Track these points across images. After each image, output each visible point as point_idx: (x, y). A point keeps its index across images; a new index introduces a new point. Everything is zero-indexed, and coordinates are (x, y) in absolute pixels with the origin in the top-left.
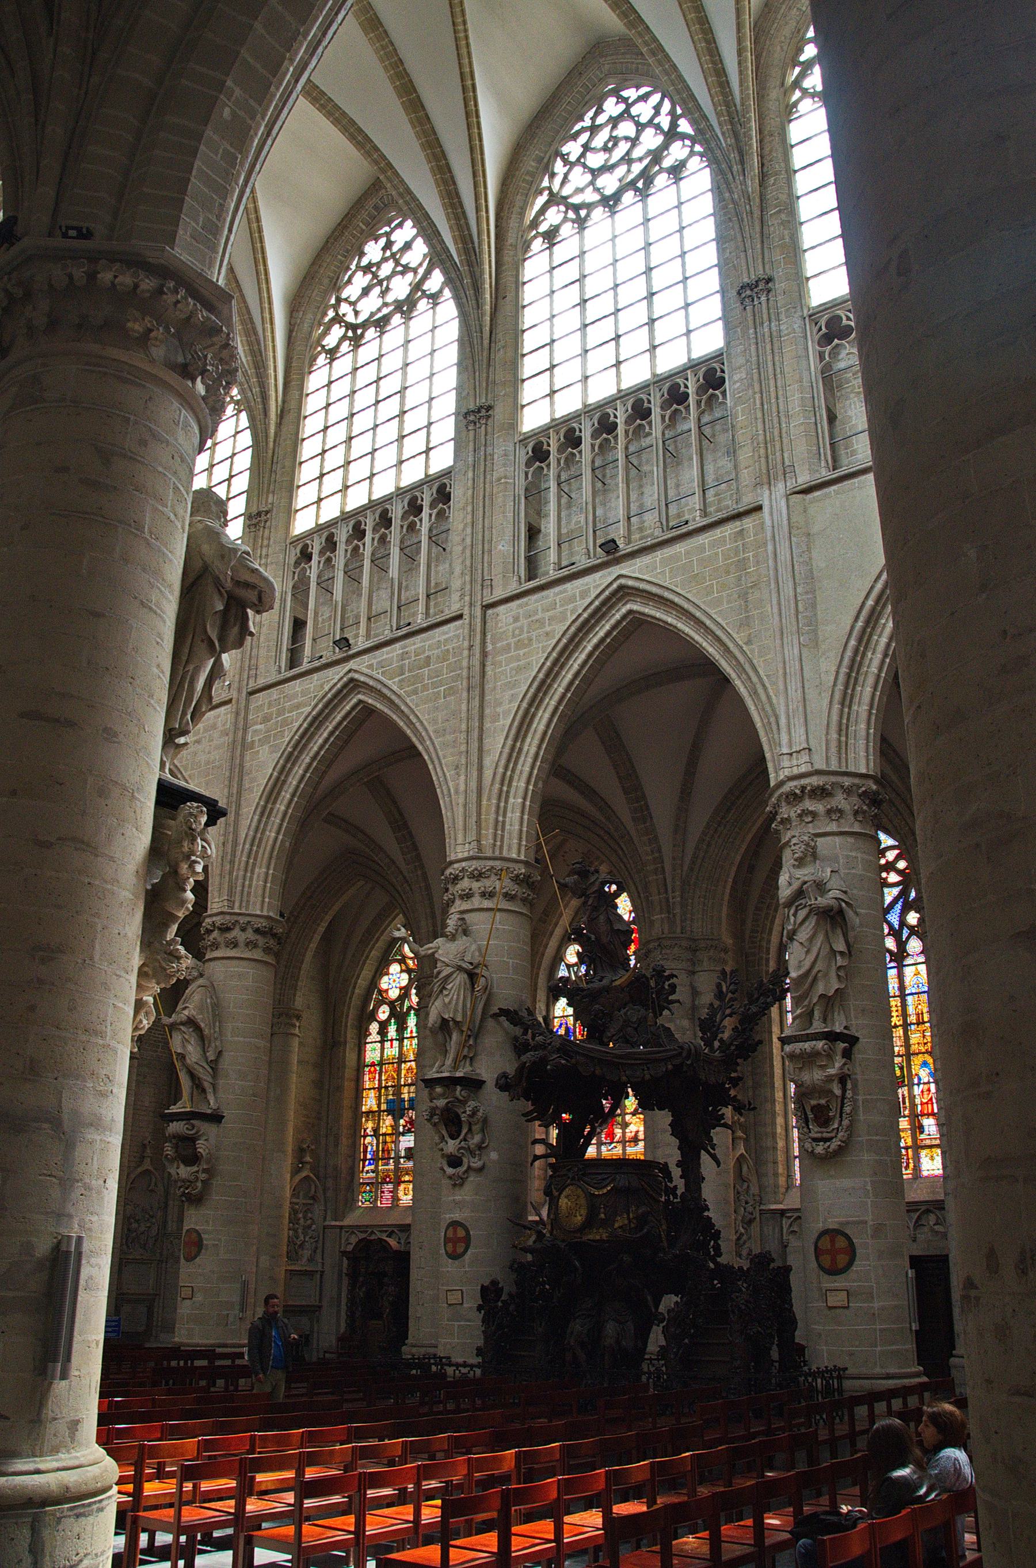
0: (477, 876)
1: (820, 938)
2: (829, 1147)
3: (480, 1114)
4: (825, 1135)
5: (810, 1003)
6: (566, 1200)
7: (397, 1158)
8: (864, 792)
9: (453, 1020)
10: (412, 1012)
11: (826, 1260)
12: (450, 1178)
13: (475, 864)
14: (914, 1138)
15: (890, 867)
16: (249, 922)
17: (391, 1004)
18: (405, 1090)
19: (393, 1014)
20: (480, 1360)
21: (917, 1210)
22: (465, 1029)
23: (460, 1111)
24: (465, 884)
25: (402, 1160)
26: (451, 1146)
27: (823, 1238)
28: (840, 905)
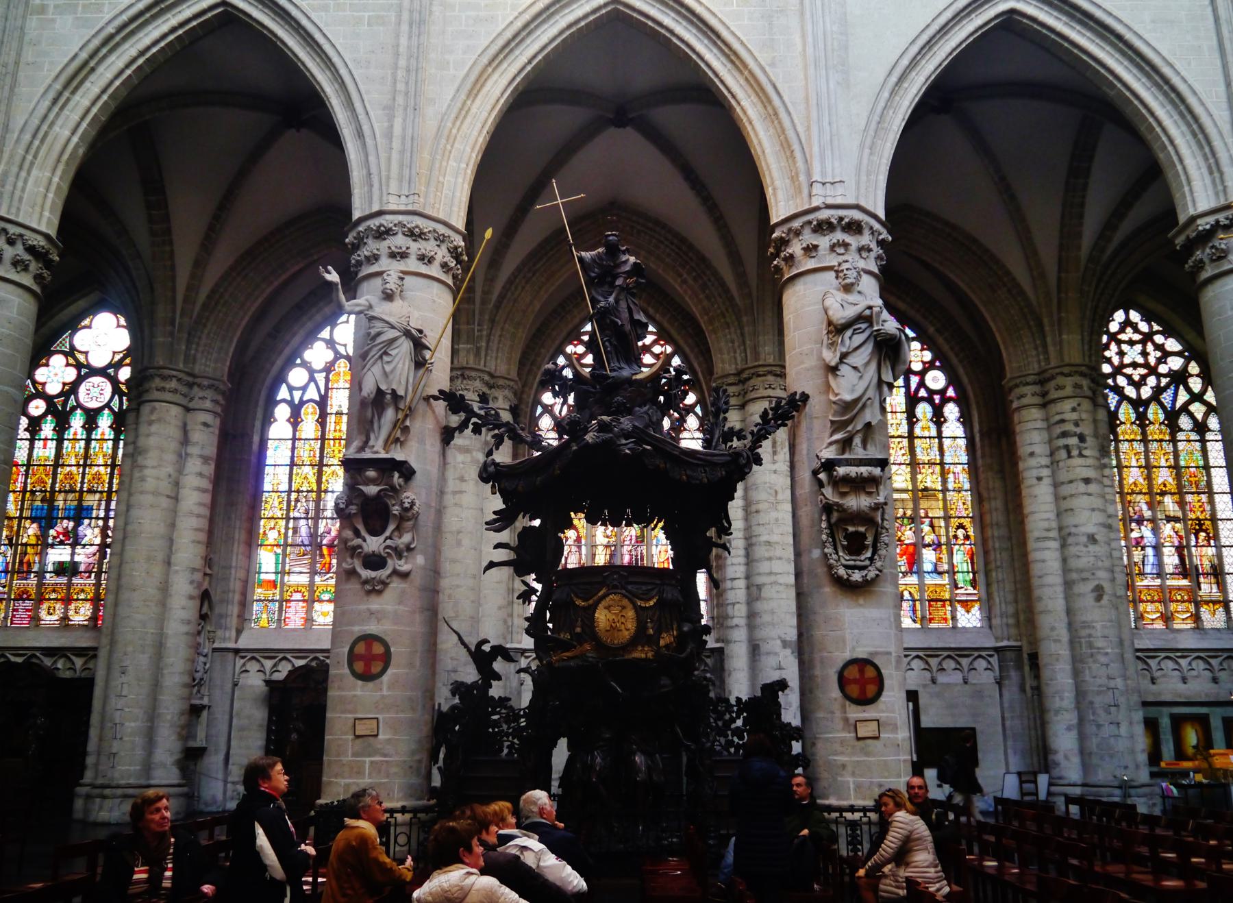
1: (873, 366)
4: (858, 563)
6: (606, 611)
7: (41, 574)
8: (883, 240)
9: (394, 391)
10: (79, 411)
11: (854, 690)
12: (366, 582)
16: (21, 236)
17: (49, 399)
19: (51, 409)
22: (402, 406)
23: (390, 502)
25: (48, 575)
26: (373, 544)
27: (850, 667)
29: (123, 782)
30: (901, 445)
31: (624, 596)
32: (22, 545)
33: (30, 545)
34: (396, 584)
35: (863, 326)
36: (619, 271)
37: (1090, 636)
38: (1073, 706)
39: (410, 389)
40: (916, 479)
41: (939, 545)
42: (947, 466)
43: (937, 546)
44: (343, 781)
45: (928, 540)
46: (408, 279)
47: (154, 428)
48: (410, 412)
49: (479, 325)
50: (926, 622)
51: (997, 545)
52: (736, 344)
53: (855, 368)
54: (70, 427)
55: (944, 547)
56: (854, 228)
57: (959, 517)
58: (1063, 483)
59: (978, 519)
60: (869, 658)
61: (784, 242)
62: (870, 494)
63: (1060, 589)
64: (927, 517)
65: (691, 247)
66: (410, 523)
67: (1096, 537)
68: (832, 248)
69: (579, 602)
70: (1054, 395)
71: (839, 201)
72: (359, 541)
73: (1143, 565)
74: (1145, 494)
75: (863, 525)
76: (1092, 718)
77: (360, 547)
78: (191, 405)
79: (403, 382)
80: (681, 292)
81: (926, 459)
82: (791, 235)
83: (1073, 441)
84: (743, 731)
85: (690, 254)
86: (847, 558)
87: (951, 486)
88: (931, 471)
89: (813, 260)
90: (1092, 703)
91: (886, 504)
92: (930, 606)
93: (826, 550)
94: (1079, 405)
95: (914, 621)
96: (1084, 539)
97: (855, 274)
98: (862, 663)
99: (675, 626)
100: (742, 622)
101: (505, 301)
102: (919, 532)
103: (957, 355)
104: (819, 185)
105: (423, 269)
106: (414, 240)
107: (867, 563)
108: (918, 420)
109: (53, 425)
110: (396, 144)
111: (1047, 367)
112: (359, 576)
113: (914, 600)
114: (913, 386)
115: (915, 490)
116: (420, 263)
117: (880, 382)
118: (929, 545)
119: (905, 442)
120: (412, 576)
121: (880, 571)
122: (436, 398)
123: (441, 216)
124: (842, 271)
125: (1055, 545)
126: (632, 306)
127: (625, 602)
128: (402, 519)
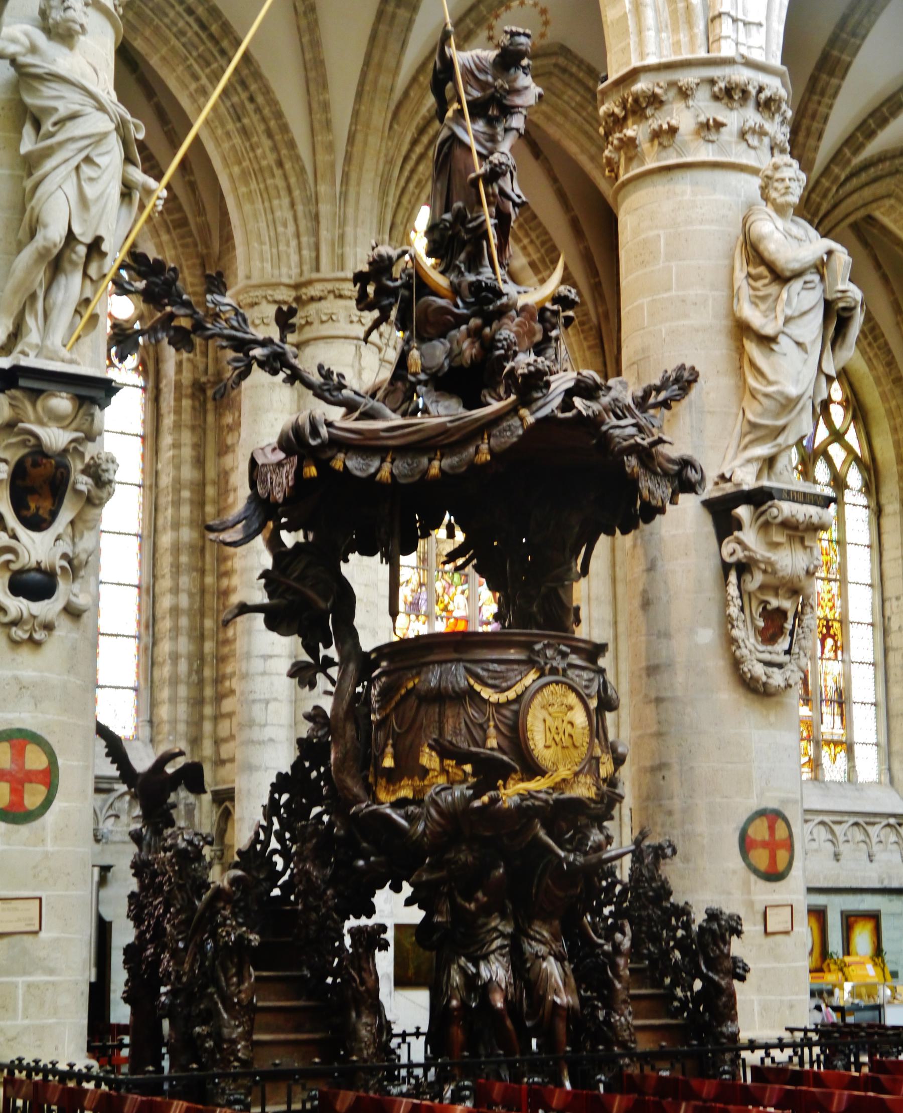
9: (98, 240)
11: (761, 858)
12: (15, 623)
27: (758, 822)
34: (64, 628)
36: (518, 101)
53: (799, 344)
60: (781, 809)
61: (655, 101)
68: (743, 135)
69: (486, 693)
82: (672, 93)
89: (710, 145)
98: (773, 816)
104: (730, 20)
124: (783, 180)
127: (572, 699)
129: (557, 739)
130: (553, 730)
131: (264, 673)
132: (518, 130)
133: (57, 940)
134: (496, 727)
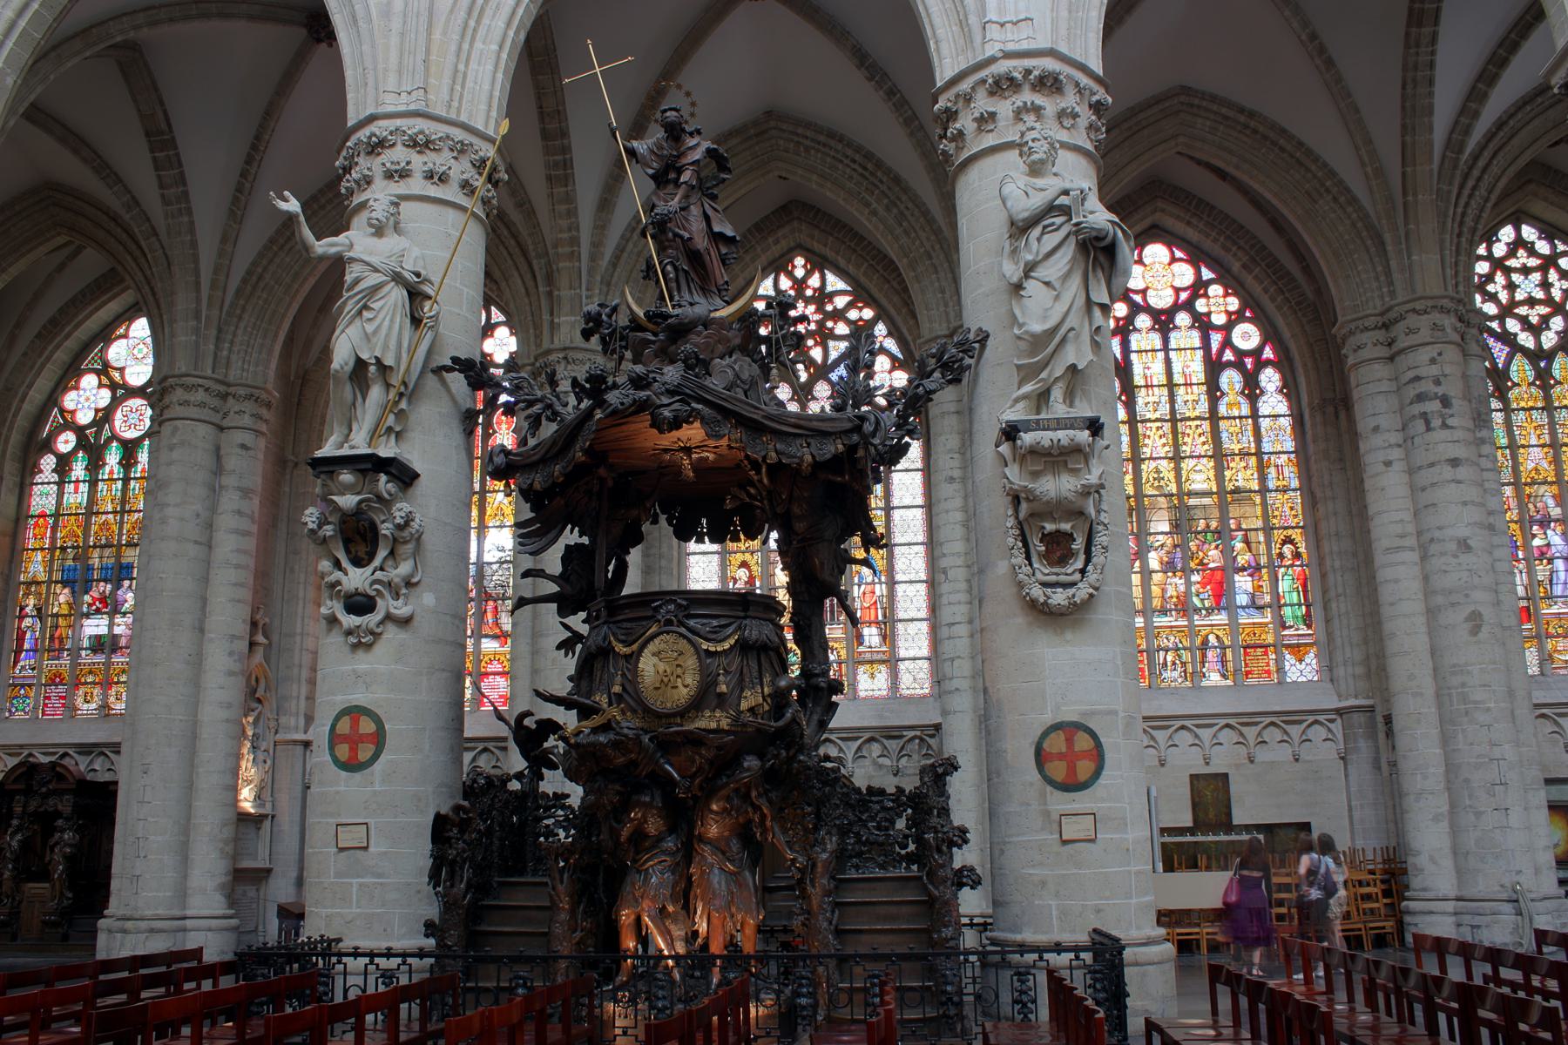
0: (420, 144)
1: (1076, 282)
2: (1074, 596)
3: (415, 525)
4: (1062, 578)
5: (1049, 376)
6: (655, 659)
7: (75, 652)
8: (1098, 102)
9: (378, 361)
10: (115, 444)
11: (1058, 770)
12: (349, 633)
13: (420, 124)
14: (850, 649)
15: (838, 315)
17: (80, 431)
18: (96, 553)
19: (82, 444)
20: (432, 942)
21: (856, 739)
22: (395, 380)
23: (378, 518)
24: (398, 155)
25: (83, 653)
26: (356, 578)
27: (1053, 735)
28: (1115, 234)
29: (148, 913)
30: (1200, 430)
31: (681, 635)
32: (53, 615)
33: (62, 616)
34: (391, 633)
35: (1059, 220)
37: (1463, 685)
38: (1442, 785)
39: (404, 355)
40: (1224, 476)
41: (1258, 568)
42: (1266, 457)
43: (1254, 570)
44: (324, 912)
45: (1242, 560)
46: (404, 206)
47: (175, 455)
48: (410, 393)
49: (588, 290)
50: (1240, 677)
51: (1337, 564)
52: (947, 295)
53: (1047, 284)
54: (105, 464)
55: (1264, 571)
56: (1049, 84)
57: (1285, 528)
58: (1420, 468)
59: (1311, 530)
61: (951, 115)
62: (1075, 472)
63: (1420, 621)
64: (1239, 529)
65: (879, 164)
66: (410, 547)
67: (1470, 542)
69: (621, 649)
70: (1403, 342)
71: (1025, 46)
72: (338, 575)
73: (1551, 584)
74: (1551, 483)
75: (1067, 521)
76: (1468, 802)
77: (338, 583)
78: (225, 423)
79: (393, 344)
80: (870, 227)
81: (1236, 448)
82: (960, 104)
83: (1433, 406)
84: (906, 837)
85: (879, 174)
86: (1047, 571)
87: (1271, 484)
88: (1243, 464)
90: (1467, 781)
91: (1102, 486)
92: (1246, 654)
93: (1013, 561)
94: (1440, 354)
95: (1224, 676)
96: (1453, 546)
97: (1046, 147)
98: (1070, 729)
99: (767, 679)
100: (964, 684)
101: (625, 255)
102: (1228, 552)
103: (1273, 300)
105: (433, 191)
106: (419, 152)
107: (1077, 576)
108: (1223, 394)
109: (85, 463)
110: (396, 24)
111: (1393, 302)
112: (340, 623)
113: (1223, 648)
114: (1215, 346)
115: (1221, 492)
116: (428, 183)
117: (1089, 303)
118: (1243, 569)
119: (1206, 425)
120: (415, 623)
121: (1096, 589)
122: (449, 369)
123: (463, 118)
125: (1414, 556)
126: (710, 212)
128: (395, 541)
129: (666, 679)
130: (661, 671)
131: (949, 638)
132: (685, 183)
133: (385, 853)
134: (623, 675)
